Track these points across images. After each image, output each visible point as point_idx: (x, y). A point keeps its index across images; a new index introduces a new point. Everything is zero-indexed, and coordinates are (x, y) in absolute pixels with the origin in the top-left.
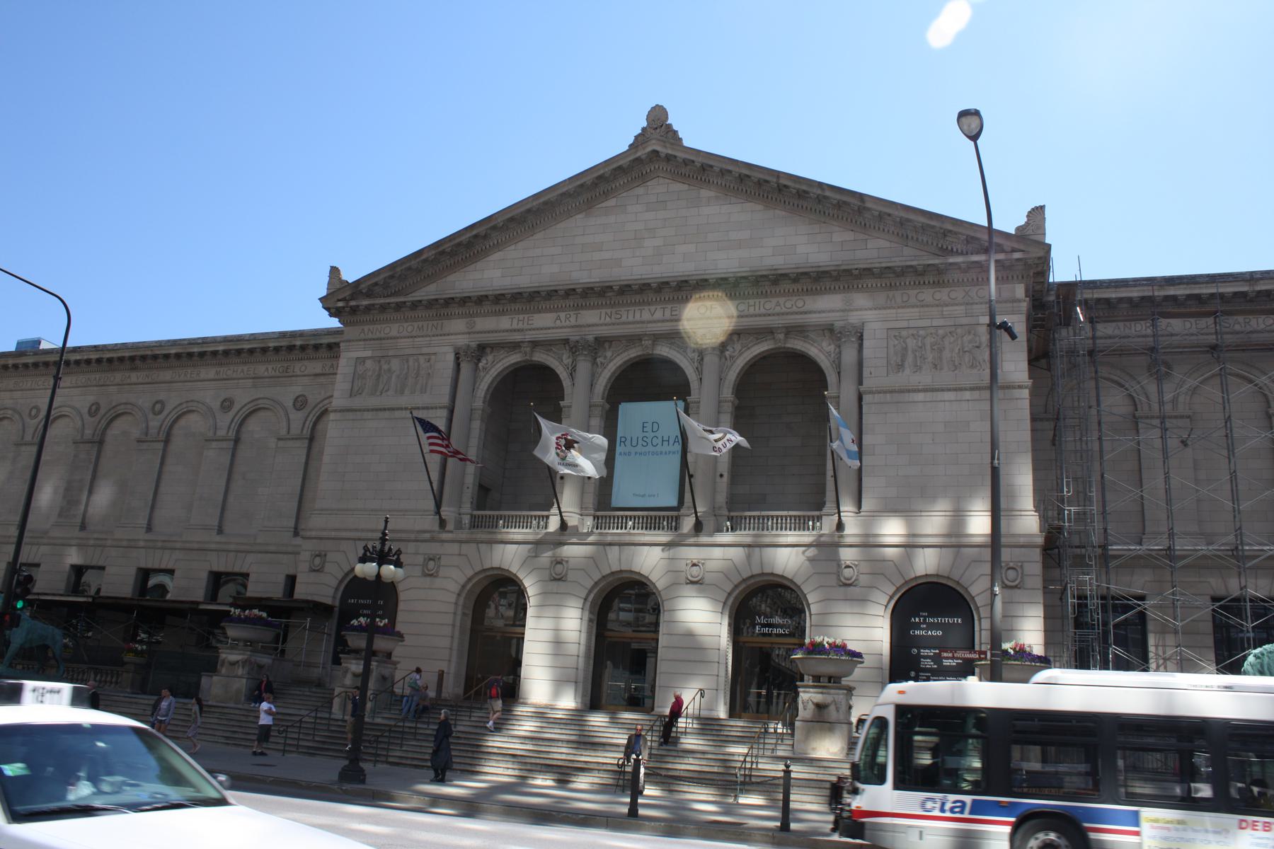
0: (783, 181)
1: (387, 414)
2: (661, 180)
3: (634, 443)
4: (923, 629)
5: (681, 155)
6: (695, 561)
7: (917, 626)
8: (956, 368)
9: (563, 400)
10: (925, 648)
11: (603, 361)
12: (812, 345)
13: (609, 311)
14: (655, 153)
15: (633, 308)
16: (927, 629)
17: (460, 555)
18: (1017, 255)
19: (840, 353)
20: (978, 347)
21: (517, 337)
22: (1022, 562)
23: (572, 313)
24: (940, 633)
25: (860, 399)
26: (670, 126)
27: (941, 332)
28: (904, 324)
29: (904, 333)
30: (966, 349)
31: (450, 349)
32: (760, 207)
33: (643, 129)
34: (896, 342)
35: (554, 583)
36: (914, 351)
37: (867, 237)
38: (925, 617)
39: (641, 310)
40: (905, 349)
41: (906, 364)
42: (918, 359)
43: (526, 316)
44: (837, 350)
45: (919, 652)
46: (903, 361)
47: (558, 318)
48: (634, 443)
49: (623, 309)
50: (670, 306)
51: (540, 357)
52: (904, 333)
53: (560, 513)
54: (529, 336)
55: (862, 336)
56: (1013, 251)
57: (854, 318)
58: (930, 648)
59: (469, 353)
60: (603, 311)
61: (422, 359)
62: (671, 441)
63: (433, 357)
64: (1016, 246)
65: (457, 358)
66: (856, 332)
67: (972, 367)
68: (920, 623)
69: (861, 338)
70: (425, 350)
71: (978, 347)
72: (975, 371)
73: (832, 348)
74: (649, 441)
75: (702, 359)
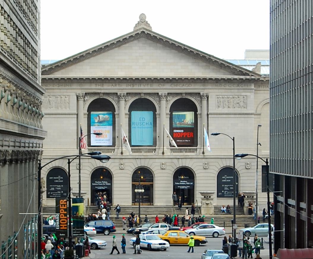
0: (185, 47)
1: (54, 116)
2: (144, 39)
3: (137, 124)
4: (225, 180)
5: (152, 34)
6: (163, 163)
7: (224, 179)
8: (234, 108)
9: (115, 112)
10: (226, 185)
11: (128, 100)
12: (193, 98)
13: (130, 84)
14: (143, 32)
15: (138, 84)
16: (226, 180)
17: (89, 162)
18: (253, 77)
19: (201, 100)
20: (241, 102)
21: (99, 91)
22: (251, 162)
23: (117, 84)
24: (230, 181)
25: (208, 115)
26: (147, 22)
27: (231, 97)
28: (220, 94)
29: (221, 96)
30: (237, 102)
31: (75, 94)
32: (177, 52)
33: (138, 22)
34: (218, 99)
35: (121, 170)
36: (223, 102)
37: (209, 65)
38: (226, 177)
39: (140, 84)
40: (220, 101)
41: (221, 106)
42: (224, 105)
43: (101, 84)
44: (201, 100)
45: (224, 185)
46: (220, 105)
47: (112, 85)
48: (137, 124)
49: (134, 84)
50: (150, 84)
51: (105, 97)
52: (221, 96)
53: (122, 149)
54: (103, 91)
55: (208, 96)
56: (252, 76)
57: (205, 92)
58: (227, 185)
59: (82, 96)
60: (128, 84)
61: (63, 97)
62: (149, 124)
63: (68, 97)
64: (253, 74)
65: (77, 97)
66: (207, 95)
67: (239, 108)
68: (225, 178)
69: (208, 98)
70: (65, 94)
71: (241, 102)
72: (239, 109)
73: (199, 99)
74: (142, 124)
75: (160, 101)
